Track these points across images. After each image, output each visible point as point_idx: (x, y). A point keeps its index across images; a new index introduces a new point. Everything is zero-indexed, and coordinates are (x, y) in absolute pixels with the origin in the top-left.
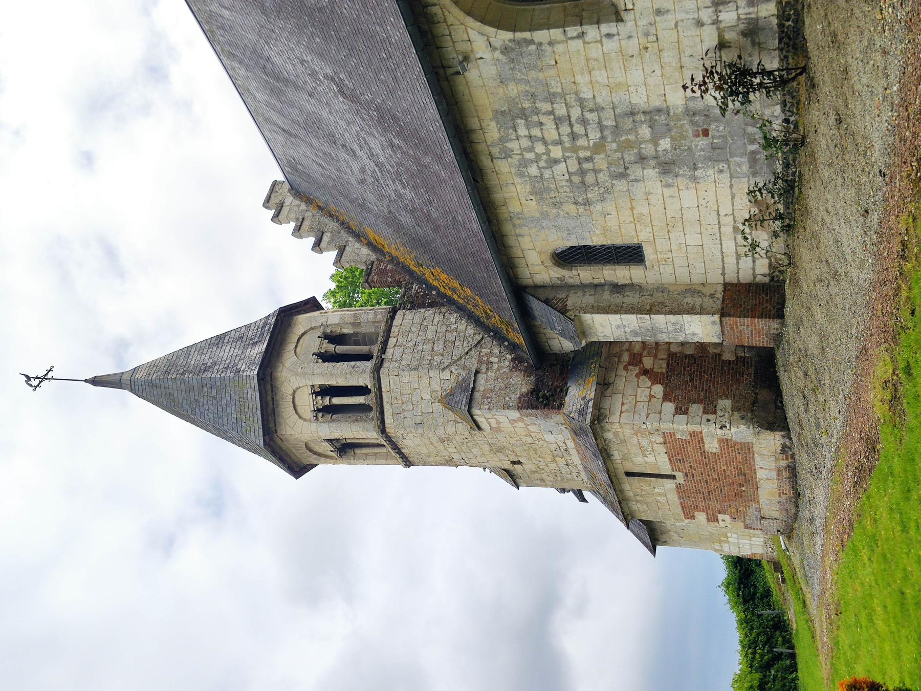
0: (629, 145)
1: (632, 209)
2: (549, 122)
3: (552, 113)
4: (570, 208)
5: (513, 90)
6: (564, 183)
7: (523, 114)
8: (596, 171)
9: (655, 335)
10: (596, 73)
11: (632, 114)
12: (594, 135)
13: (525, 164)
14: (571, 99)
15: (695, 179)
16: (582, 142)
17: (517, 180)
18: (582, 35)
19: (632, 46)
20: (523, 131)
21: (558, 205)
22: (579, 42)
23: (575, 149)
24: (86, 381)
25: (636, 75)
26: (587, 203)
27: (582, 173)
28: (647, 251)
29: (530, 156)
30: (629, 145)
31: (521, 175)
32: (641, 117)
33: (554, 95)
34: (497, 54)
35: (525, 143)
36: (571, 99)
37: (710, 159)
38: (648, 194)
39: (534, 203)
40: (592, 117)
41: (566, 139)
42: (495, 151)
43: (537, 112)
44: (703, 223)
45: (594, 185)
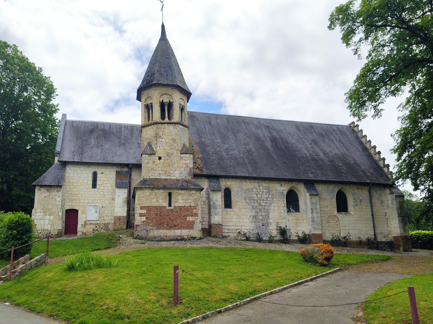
0: (261, 210)
2: (267, 196)
3: (269, 197)
4: (244, 195)
5: (274, 191)
6: (251, 196)
7: (268, 192)
8: (254, 203)
9: (214, 208)
10: (277, 207)
11: (268, 212)
12: (263, 204)
13: (256, 189)
14: (272, 202)
15: (252, 222)
16: (261, 201)
17: (252, 186)
18: (285, 206)
19: (282, 215)
20: (265, 191)
21: (245, 193)
22: (283, 206)
23: (260, 200)
25: (276, 214)
26: (245, 199)
27: (254, 200)
28: (229, 210)
29: (259, 190)
30: (261, 210)
31: (254, 187)
32: (267, 214)
33: (273, 199)
34: (282, 191)
35: (262, 190)
36: (272, 202)
37: (257, 225)
38: (248, 212)
39: (246, 188)
40: (268, 205)
41: (263, 199)
42: (260, 184)
43: (269, 195)
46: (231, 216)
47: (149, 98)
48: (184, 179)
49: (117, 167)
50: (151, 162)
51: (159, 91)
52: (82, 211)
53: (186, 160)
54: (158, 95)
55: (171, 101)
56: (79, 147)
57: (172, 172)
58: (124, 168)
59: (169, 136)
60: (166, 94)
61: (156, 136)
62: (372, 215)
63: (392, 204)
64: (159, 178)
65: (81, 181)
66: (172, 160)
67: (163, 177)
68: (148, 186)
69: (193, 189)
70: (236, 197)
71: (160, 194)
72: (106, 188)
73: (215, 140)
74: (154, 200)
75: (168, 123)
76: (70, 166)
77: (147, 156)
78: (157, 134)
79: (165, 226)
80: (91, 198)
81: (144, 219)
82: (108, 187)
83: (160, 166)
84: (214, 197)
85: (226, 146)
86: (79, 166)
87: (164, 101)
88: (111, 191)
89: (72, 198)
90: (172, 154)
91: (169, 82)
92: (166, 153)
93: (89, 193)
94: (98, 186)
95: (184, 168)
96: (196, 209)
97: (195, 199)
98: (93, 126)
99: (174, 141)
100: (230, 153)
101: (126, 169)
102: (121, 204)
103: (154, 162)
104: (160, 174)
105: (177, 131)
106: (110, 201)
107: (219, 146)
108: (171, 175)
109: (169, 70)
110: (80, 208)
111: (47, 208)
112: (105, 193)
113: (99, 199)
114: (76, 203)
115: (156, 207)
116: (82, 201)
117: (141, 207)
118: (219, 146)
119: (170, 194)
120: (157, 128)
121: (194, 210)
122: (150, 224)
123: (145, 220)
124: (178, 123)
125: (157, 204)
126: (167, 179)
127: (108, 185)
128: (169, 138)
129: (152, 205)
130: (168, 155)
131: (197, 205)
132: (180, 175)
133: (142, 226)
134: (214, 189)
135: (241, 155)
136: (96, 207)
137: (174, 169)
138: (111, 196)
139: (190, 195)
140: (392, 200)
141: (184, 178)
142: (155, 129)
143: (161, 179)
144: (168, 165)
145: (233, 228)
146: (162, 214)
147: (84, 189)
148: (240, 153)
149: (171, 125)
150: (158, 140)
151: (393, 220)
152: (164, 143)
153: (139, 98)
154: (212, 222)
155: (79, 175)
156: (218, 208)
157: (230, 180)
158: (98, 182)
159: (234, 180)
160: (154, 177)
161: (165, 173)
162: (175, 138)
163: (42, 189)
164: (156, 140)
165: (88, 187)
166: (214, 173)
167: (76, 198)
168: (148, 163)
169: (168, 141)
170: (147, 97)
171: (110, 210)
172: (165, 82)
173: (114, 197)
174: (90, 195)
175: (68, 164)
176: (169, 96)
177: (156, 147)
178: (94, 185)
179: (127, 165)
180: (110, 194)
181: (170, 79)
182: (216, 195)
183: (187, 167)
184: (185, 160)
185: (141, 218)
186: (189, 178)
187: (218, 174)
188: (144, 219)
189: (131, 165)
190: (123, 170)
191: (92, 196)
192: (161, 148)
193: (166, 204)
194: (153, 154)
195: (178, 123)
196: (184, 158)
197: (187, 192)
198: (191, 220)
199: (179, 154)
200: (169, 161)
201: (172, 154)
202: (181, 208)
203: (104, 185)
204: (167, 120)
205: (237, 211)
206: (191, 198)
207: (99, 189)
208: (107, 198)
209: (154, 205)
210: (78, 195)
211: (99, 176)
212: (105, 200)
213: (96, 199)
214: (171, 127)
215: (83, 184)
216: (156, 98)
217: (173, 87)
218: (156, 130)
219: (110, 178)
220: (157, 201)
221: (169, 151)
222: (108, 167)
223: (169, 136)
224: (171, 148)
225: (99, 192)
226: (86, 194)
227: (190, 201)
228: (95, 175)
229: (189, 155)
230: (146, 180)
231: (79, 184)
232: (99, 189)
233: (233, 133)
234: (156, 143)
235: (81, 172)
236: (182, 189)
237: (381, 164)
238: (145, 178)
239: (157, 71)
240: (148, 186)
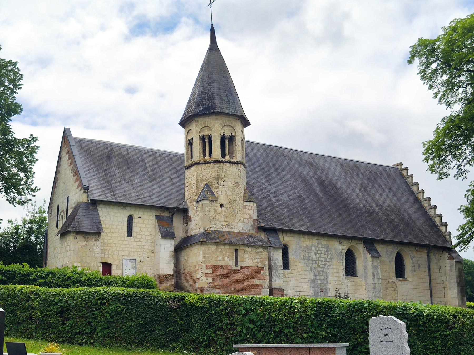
0: (319, 273)
1: (302, 270)
2: (326, 256)
3: (328, 258)
4: (302, 254)
5: (333, 251)
6: (310, 255)
7: (327, 251)
8: (313, 264)
9: (275, 269)
10: (336, 270)
11: (327, 276)
12: (322, 266)
13: (315, 247)
14: (330, 263)
15: (310, 287)
16: (320, 262)
17: (311, 243)
18: (344, 269)
19: (341, 279)
20: (323, 249)
21: (303, 251)
22: (342, 269)
23: (318, 260)
24: (212, 25)
25: (335, 278)
26: (304, 259)
27: (312, 260)
28: (287, 271)
29: (317, 249)
30: (319, 273)
31: (312, 245)
32: (326, 277)
33: (332, 260)
34: (341, 250)
35: (321, 249)
36: (330, 263)
37: (315, 291)
38: (306, 275)
39: (304, 245)
40: (326, 266)
41: (321, 259)
42: (319, 241)
43: (328, 254)
44: (297, 287)
45: (309, 262)
46: (289, 279)
47: (206, 128)
48: (248, 233)
49: (157, 210)
50: (212, 210)
51: (221, 122)
52: (117, 265)
53: (249, 210)
54: (219, 125)
55: (233, 134)
56: (104, 180)
57: (234, 224)
58: (164, 212)
59: (232, 178)
60: (228, 125)
61: (218, 178)
62: (430, 283)
63: (451, 270)
64: (222, 230)
65: (114, 227)
66: (235, 209)
67: (225, 229)
68: (214, 241)
69: (260, 246)
70: (294, 256)
71: (226, 251)
72: (144, 237)
73: (259, 180)
74: (220, 258)
75: (230, 163)
76: (101, 206)
77: (208, 202)
78: (218, 175)
79: (232, 289)
80: (126, 249)
81: (210, 280)
82: (146, 235)
83: (222, 216)
84: (274, 256)
85: (273, 189)
86: (112, 207)
87: (225, 134)
88: (149, 241)
89: (105, 248)
90: (235, 201)
91: (233, 111)
92: (228, 200)
93: (125, 243)
94: (134, 234)
95: (248, 219)
96: (263, 270)
97: (262, 258)
98: (107, 148)
99: (237, 185)
100: (280, 199)
101: (166, 214)
102: (167, 259)
103: (216, 211)
104: (222, 225)
105: (240, 173)
106: (149, 254)
107: (266, 189)
108: (233, 227)
109: (230, 95)
110: (114, 262)
111: (84, 261)
112: (143, 244)
113: (136, 251)
114: (109, 254)
115: (222, 266)
116: (116, 253)
117: (206, 265)
118: (266, 189)
119: (236, 251)
120: (218, 167)
121: (261, 272)
122: (217, 287)
123: (211, 281)
124: (241, 163)
125: (223, 263)
126: (230, 232)
127: (146, 233)
128: (231, 181)
129: (218, 264)
130: (231, 202)
131: (265, 266)
132: (243, 227)
133: (209, 289)
134: (276, 246)
135: (293, 202)
136: (133, 261)
137: (237, 221)
138: (150, 248)
139: (257, 253)
140: (451, 266)
141: (248, 232)
142: (216, 168)
143: (224, 232)
144: (230, 215)
145: (291, 293)
146: (229, 275)
147: (118, 237)
148: (291, 200)
149: (233, 165)
150: (219, 183)
151: (450, 289)
152: (226, 187)
153: (184, 123)
154: (273, 287)
155: (112, 219)
156: (279, 270)
157: (288, 235)
158: (135, 229)
159: (292, 235)
160: (216, 229)
161: (227, 225)
162: (237, 181)
163: (78, 236)
164: (218, 183)
165: (122, 234)
166: (272, 226)
167: (108, 248)
168: (209, 211)
169: (230, 184)
170: (203, 126)
171: (149, 265)
172: (229, 111)
173: (153, 248)
174: (125, 245)
175: (99, 204)
176: (231, 128)
177: (218, 192)
178: (130, 233)
179: (168, 209)
180: (148, 244)
181: (233, 107)
182: (277, 253)
183: (251, 218)
184: (248, 209)
185: (207, 279)
186: (253, 232)
187: (277, 227)
188: (210, 280)
189: (175, 209)
190: (163, 215)
191: (128, 246)
192: (223, 192)
193: (232, 263)
194: (214, 200)
195: (241, 163)
196: (247, 207)
197: (254, 250)
198: (259, 283)
199: (242, 202)
200: (232, 210)
201: (235, 201)
202: (248, 268)
203: (142, 233)
204: (227, 158)
205: (295, 273)
206: (258, 257)
207: (136, 237)
208: (145, 250)
209: (220, 264)
210: (112, 245)
211: (135, 221)
212: (142, 252)
213: (132, 250)
214: (234, 167)
215: (117, 231)
216: (218, 130)
217: (235, 118)
218: (217, 170)
219: (148, 224)
220: (224, 259)
221: (231, 198)
222: (146, 210)
223: (232, 178)
224: (234, 195)
225: (136, 242)
226: (120, 244)
227: (257, 260)
228: (130, 219)
229: (253, 203)
230: (209, 233)
231: (113, 231)
232: (136, 237)
233: (276, 170)
234: (218, 187)
235: (115, 215)
236: (248, 246)
237: (436, 221)
238: (207, 229)
239: (217, 95)
240: (214, 241)
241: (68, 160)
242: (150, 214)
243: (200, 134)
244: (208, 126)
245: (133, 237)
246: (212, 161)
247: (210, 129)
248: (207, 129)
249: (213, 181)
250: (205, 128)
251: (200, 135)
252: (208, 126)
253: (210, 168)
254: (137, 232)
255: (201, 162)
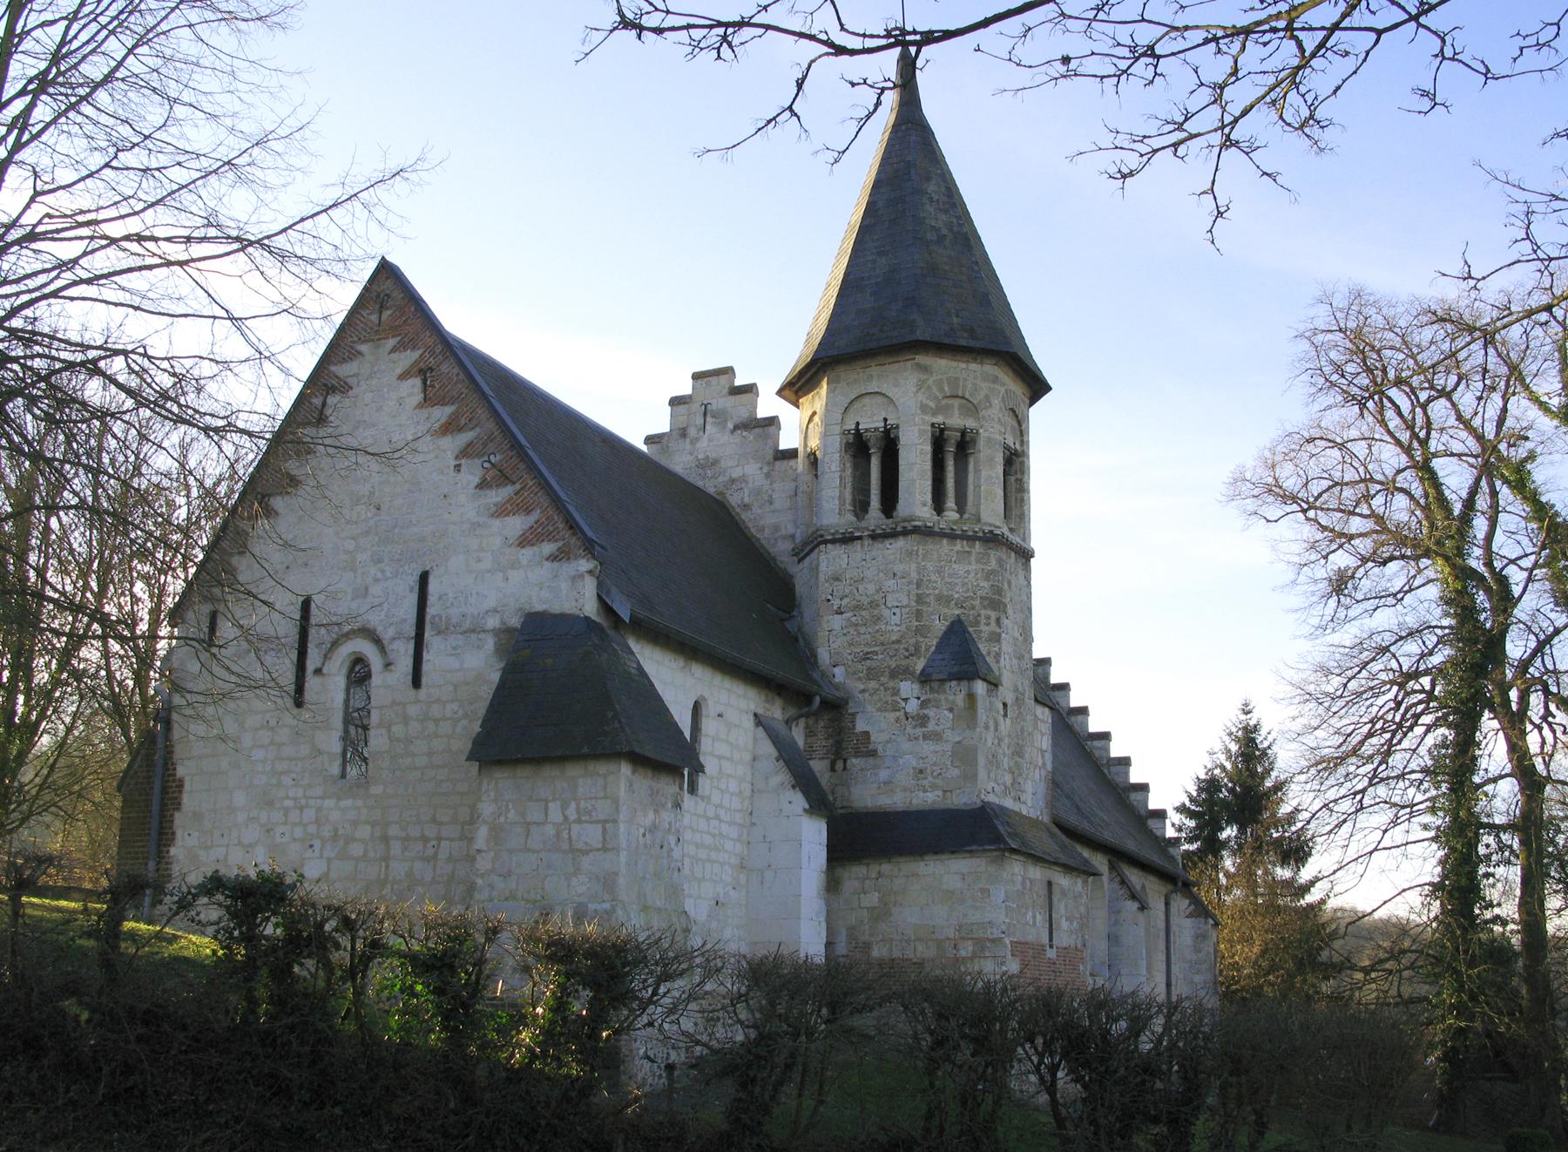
47: (956, 403)
88: (738, 818)
208: (726, 856)
232: (705, 798)
241: (420, 406)
242: (743, 704)
243: (935, 420)
244: (963, 398)
245: (703, 798)
246: (981, 534)
247: (972, 409)
248: (961, 407)
249: (983, 612)
250: (950, 401)
251: (933, 425)
252: (963, 398)
253: (973, 559)
254: (712, 778)
255: (936, 529)
